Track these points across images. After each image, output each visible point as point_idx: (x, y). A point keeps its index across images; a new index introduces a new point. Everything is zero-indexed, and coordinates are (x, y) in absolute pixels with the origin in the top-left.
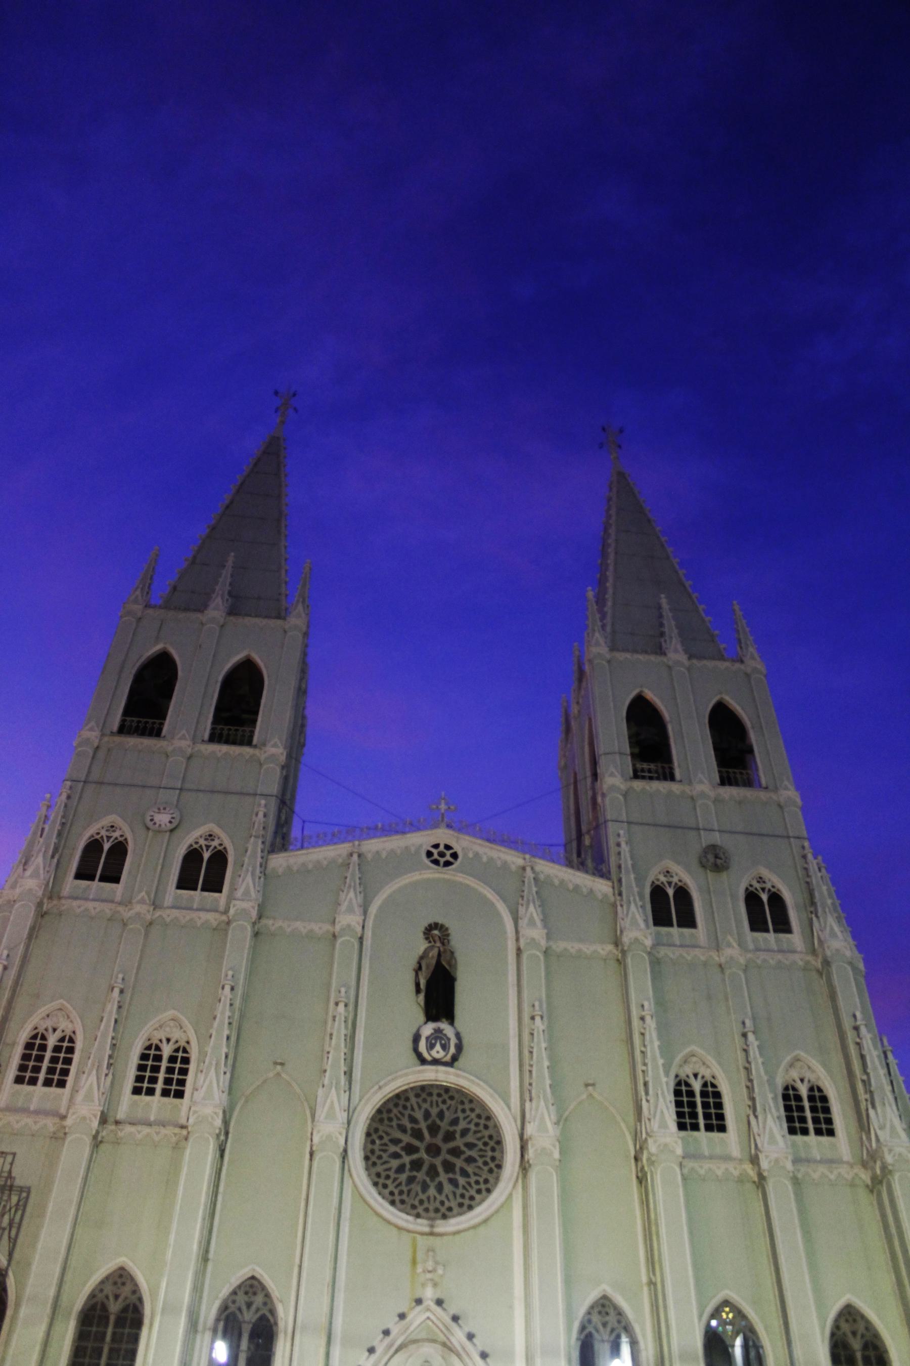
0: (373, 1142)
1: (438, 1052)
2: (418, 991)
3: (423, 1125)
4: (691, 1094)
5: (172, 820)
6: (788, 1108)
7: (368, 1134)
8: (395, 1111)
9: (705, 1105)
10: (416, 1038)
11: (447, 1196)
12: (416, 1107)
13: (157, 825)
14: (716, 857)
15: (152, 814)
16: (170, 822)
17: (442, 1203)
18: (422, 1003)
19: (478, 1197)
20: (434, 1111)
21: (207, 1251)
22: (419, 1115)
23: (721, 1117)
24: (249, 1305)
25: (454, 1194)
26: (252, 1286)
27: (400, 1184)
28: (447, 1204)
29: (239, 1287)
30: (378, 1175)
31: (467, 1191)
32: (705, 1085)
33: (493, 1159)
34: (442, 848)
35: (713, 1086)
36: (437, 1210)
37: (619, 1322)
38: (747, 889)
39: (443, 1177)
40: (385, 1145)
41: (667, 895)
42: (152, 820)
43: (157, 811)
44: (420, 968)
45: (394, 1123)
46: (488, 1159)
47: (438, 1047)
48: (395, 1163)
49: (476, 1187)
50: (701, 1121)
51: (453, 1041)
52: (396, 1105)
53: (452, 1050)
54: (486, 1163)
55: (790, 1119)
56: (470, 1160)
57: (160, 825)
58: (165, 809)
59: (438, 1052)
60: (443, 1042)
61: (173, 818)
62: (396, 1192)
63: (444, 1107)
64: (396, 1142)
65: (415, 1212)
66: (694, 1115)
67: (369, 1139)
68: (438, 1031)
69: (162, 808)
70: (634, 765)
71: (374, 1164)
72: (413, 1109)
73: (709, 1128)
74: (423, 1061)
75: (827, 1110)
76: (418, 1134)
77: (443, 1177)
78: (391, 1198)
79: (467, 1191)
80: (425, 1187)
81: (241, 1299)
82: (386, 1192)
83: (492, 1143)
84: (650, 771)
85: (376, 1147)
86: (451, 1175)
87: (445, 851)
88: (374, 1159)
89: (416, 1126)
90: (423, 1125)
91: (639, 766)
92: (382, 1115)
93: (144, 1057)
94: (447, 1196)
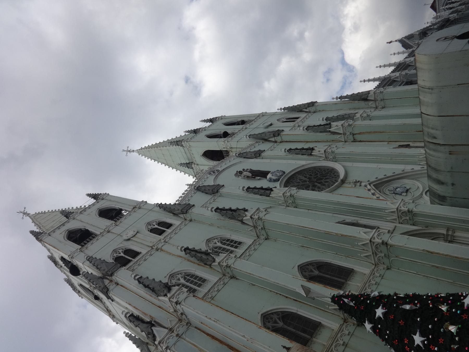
32: (185, 279)
35: (188, 276)
38: (148, 231)
41: (122, 257)
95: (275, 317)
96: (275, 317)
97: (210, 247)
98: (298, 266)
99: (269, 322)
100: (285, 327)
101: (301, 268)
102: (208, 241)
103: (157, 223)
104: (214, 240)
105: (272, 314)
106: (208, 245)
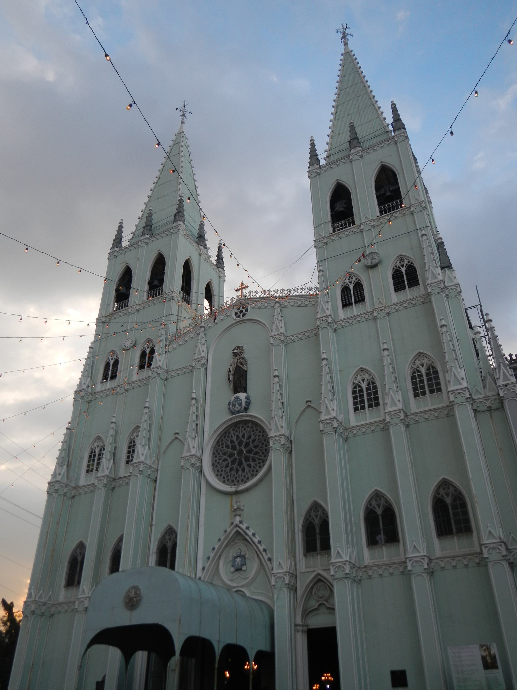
0: (216, 457)
1: (237, 408)
2: (230, 381)
3: (236, 443)
4: (361, 391)
5: (132, 342)
6: (414, 383)
7: (214, 454)
8: (224, 440)
9: (369, 395)
10: (229, 404)
11: (247, 473)
12: (233, 435)
13: (127, 347)
14: (372, 259)
15: (125, 342)
16: (131, 343)
17: (245, 476)
18: (232, 387)
19: (259, 470)
20: (240, 435)
21: (152, 521)
22: (235, 438)
23: (377, 399)
24: (170, 539)
25: (250, 471)
26: (171, 532)
27: (227, 473)
28: (247, 476)
29: (166, 533)
30: (218, 471)
31: (255, 468)
32: (369, 384)
33: (266, 450)
34: (241, 309)
35: (373, 383)
36: (242, 480)
37: (324, 514)
38: (394, 269)
39: (245, 464)
40: (221, 456)
42: (125, 345)
43: (126, 340)
44: (230, 371)
45: (224, 446)
46: (264, 451)
47: (237, 406)
48: (225, 463)
49: (258, 465)
50: (366, 404)
51: (244, 400)
52: (225, 437)
53: (244, 404)
54: (263, 453)
55: (415, 389)
56: (257, 453)
57: (128, 346)
58: (129, 338)
59: (237, 408)
60: (239, 402)
61: (132, 341)
62: (226, 477)
63: (245, 432)
64: (224, 454)
65: (233, 483)
66: (362, 402)
67: (214, 456)
68: (237, 398)
69: (128, 338)
70: (333, 226)
71: (216, 466)
72: (232, 437)
73: (370, 406)
74: (233, 413)
75: (437, 378)
76: (234, 448)
77: (245, 464)
78: (223, 480)
79: (255, 468)
80: (237, 471)
81: (167, 537)
82: (222, 477)
83: (265, 443)
84: (342, 225)
85: (217, 458)
86: (248, 463)
87: (243, 309)
88: (216, 464)
89: (233, 444)
90: (236, 443)
91: (336, 225)
92: (218, 443)
93: (130, 447)
94: (246, 473)
95: (383, 502)
96: (383, 502)
97: (415, 365)
98: (444, 479)
99: (376, 500)
100: (380, 517)
101: (444, 481)
102: (419, 355)
103: (409, 264)
104: (425, 358)
105: (384, 497)
106: (416, 360)
